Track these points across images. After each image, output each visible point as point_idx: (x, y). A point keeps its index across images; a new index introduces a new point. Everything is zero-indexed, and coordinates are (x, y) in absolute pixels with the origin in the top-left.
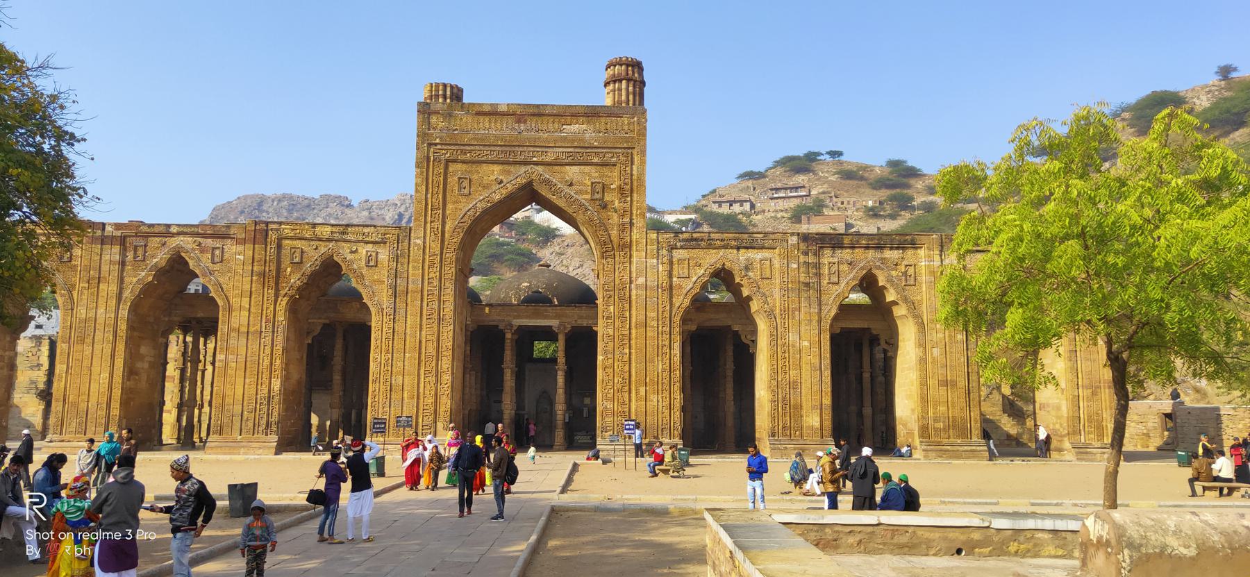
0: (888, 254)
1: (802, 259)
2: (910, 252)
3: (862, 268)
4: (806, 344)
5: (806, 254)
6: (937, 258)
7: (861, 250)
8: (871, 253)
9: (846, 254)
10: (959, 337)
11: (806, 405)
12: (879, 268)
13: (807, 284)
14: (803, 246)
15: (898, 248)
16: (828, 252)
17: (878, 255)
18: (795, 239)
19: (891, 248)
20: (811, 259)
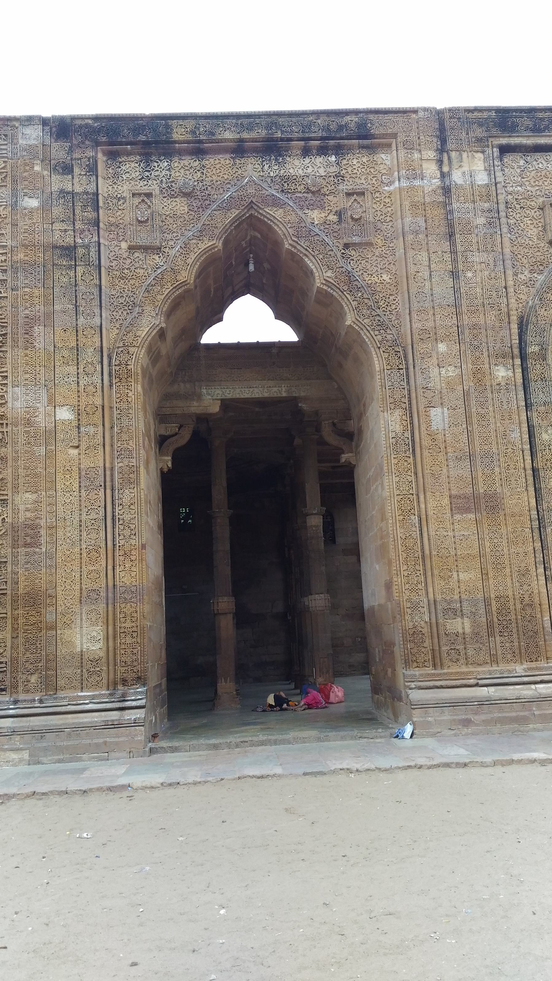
0: (298, 166)
1: (57, 183)
2: (356, 162)
3: (226, 207)
4: (65, 414)
5: (67, 169)
6: (431, 168)
7: (224, 160)
8: (252, 169)
9: (182, 170)
10: (501, 373)
11: (66, 593)
12: (276, 203)
13: (69, 251)
14: (59, 151)
15: (323, 151)
16: (131, 167)
17: (272, 169)
18: (33, 136)
19: (306, 152)
20: (79, 184)
